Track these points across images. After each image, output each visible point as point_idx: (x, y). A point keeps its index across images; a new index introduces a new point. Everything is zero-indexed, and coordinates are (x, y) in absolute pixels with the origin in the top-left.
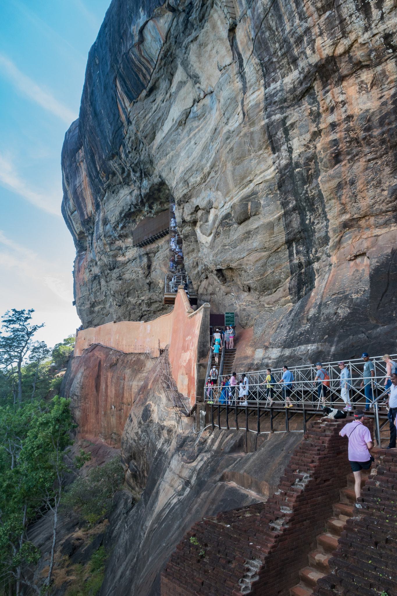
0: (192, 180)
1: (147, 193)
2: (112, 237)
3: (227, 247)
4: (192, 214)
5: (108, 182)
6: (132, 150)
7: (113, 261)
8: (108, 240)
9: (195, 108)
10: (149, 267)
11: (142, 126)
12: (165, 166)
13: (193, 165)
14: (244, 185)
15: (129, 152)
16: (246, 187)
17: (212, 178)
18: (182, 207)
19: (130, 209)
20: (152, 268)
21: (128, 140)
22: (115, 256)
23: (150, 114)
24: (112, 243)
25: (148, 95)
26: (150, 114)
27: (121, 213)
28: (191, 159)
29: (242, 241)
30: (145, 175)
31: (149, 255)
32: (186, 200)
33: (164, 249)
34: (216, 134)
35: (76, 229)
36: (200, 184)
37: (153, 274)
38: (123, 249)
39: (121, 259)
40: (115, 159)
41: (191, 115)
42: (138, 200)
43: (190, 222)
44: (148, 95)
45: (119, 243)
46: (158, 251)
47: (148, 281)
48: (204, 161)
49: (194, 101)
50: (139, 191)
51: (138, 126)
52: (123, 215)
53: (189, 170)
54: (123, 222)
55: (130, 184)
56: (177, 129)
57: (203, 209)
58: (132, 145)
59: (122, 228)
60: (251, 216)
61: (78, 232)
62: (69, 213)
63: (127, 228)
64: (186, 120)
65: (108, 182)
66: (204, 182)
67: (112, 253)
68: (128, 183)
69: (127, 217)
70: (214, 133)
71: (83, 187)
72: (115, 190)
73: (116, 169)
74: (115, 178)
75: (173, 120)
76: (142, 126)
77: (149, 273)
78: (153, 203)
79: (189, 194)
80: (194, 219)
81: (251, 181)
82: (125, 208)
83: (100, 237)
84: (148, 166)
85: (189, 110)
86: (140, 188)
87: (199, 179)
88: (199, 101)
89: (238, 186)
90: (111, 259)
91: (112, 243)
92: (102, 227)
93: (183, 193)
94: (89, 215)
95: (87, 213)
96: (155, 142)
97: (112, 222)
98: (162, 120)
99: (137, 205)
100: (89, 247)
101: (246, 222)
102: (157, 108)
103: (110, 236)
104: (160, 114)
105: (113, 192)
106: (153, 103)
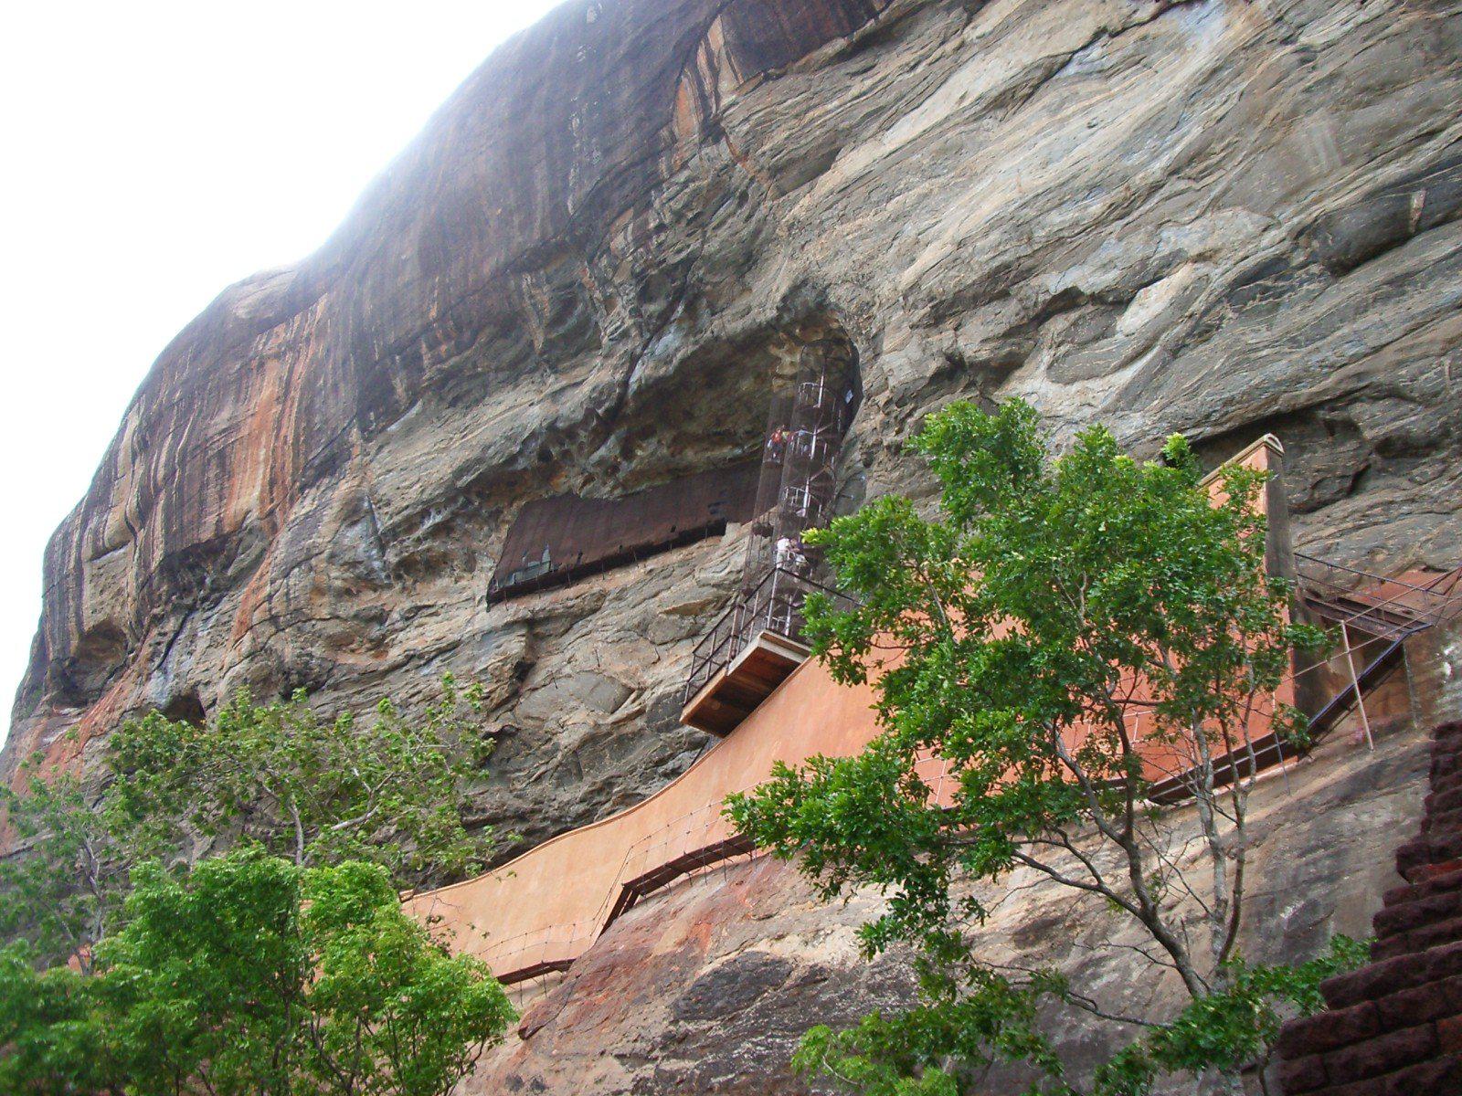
0: (1056, 219)
1: (660, 381)
2: (361, 569)
3: (1264, 353)
4: (1010, 333)
5: (452, 361)
6: (678, 222)
7: (324, 659)
8: (336, 576)
9: (1096, 52)
10: (523, 670)
11: (779, 136)
12: (862, 238)
13: (1074, 177)
14: (1393, 153)
15: (661, 228)
16: (1398, 156)
17: (1168, 198)
18: (950, 324)
19: (513, 459)
20: (538, 678)
21: (675, 189)
22: (338, 643)
23: (836, 103)
24: (348, 592)
25: (842, 57)
26: (829, 107)
27: (460, 473)
28: (1053, 169)
29: (1361, 309)
30: (691, 311)
31: (539, 630)
32: (1001, 286)
33: (631, 598)
34: (1213, 82)
35: (87, 613)
36: (1099, 222)
37: (531, 704)
38: (395, 616)
39: (362, 660)
40: (550, 270)
41: (1071, 69)
42: (600, 404)
43: (983, 366)
44: (842, 57)
45: (368, 601)
46: (594, 611)
47: (494, 727)
48: (1135, 159)
49: (1097, 36)
50: (625, 369)
51: (759, 133)
52: (467, 479)
53: (1048, 191)
54: (453, 508)
55: (561, 367)
56: (977, 118)
57: (1096, 298)
58: (687, 206)
59: (436, 531)
60: (1419, 231)
61: (88, 624)
62: (87, 551)
63: (456, 536)
64: (1036, 87)
65: (452, 361)
66: (1121, 218)
67: (334, 628)
68: (559, 360)
69: (479, 494)
70: (1205, 81)
71: (245, 432)
72: (468, 392)
73: (534, 305)
74: (499, 344)
75: (962, 98)
76: (779, 136)
77: (515, 694)
78: (646, 433)
79: (1029, 263)
80: (1010, 353)
81: (1432, 134)
82: (491, 451)
83: (308, 559)
84: (727, 277)
85: (1060, 59)
86: (633, 360)
87: (1096, 207)
88: (1124, 30)
89: (1361, 160)
90: (317, 650)
91: (348, 592)
92: (334, 526)
93: (995, 264)
94: (227, 529)
95: (220, 521)
96: (822, 178)
97: (399, 503)
98: (883, 116)
99: (571, 433)
100: (151, 660)
101: (1389, 256)
102: (871, 89)
103: (354, 564)
104: (883, 101)
105: (453, 404)
106: (860, 78)
